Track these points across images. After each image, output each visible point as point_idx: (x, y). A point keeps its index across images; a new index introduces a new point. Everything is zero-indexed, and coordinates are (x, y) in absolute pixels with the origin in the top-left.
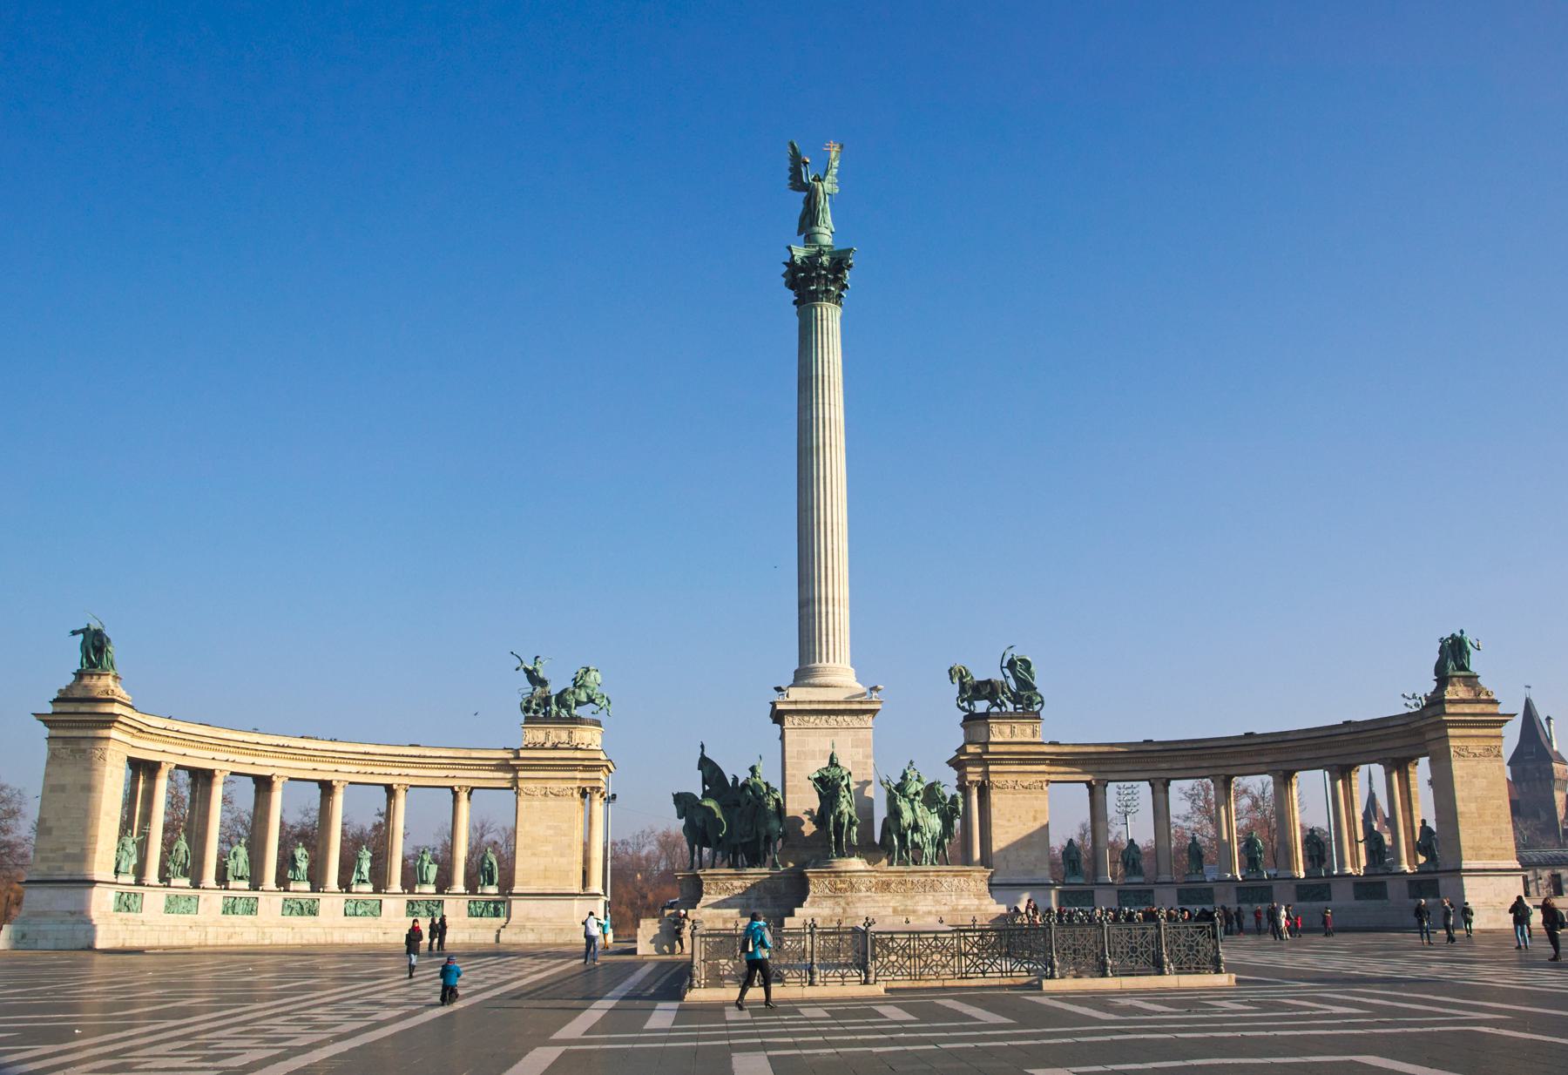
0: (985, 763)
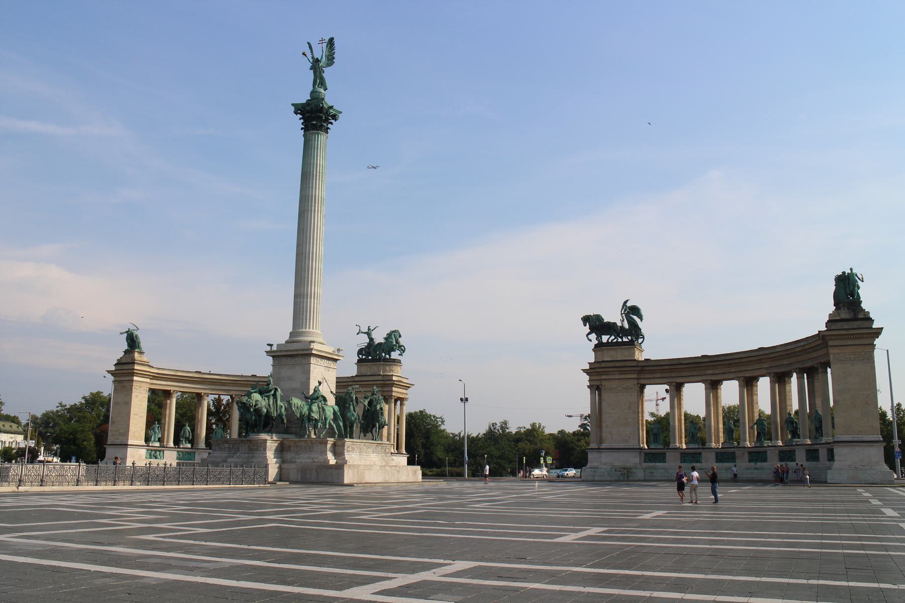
0: (599, 374)
